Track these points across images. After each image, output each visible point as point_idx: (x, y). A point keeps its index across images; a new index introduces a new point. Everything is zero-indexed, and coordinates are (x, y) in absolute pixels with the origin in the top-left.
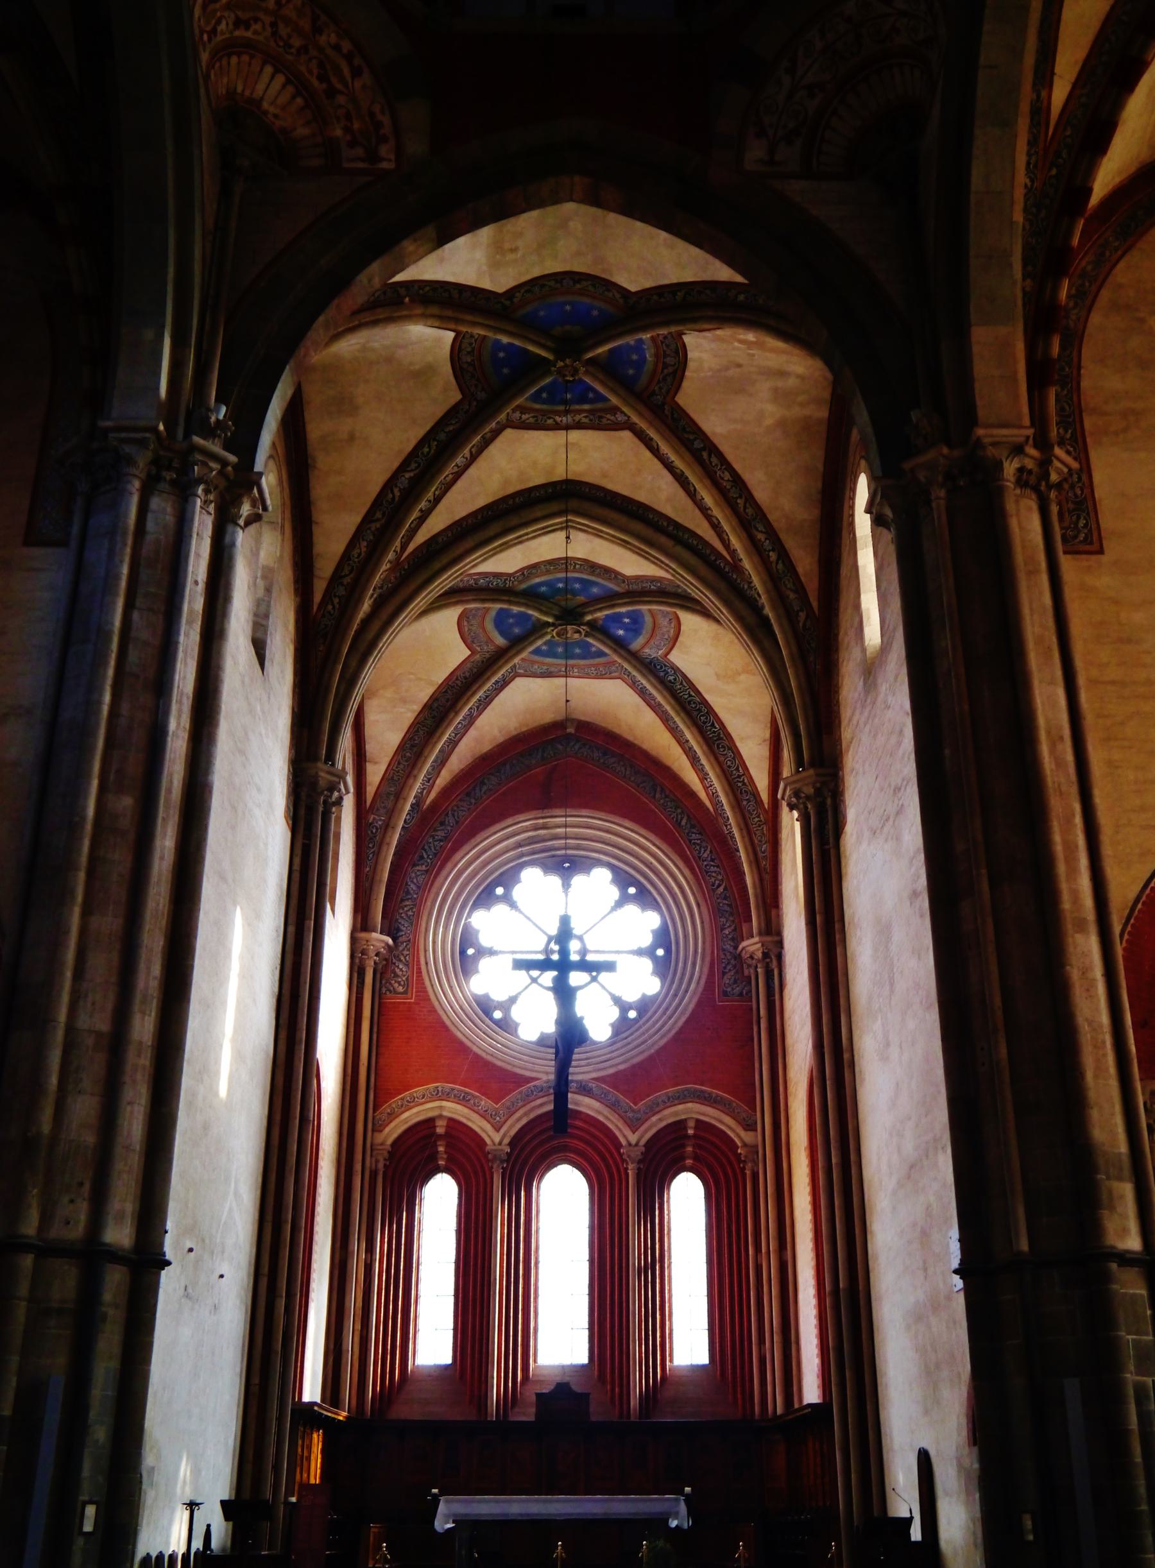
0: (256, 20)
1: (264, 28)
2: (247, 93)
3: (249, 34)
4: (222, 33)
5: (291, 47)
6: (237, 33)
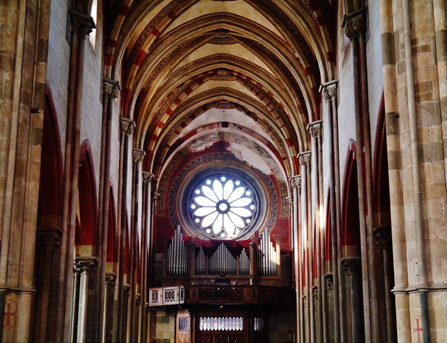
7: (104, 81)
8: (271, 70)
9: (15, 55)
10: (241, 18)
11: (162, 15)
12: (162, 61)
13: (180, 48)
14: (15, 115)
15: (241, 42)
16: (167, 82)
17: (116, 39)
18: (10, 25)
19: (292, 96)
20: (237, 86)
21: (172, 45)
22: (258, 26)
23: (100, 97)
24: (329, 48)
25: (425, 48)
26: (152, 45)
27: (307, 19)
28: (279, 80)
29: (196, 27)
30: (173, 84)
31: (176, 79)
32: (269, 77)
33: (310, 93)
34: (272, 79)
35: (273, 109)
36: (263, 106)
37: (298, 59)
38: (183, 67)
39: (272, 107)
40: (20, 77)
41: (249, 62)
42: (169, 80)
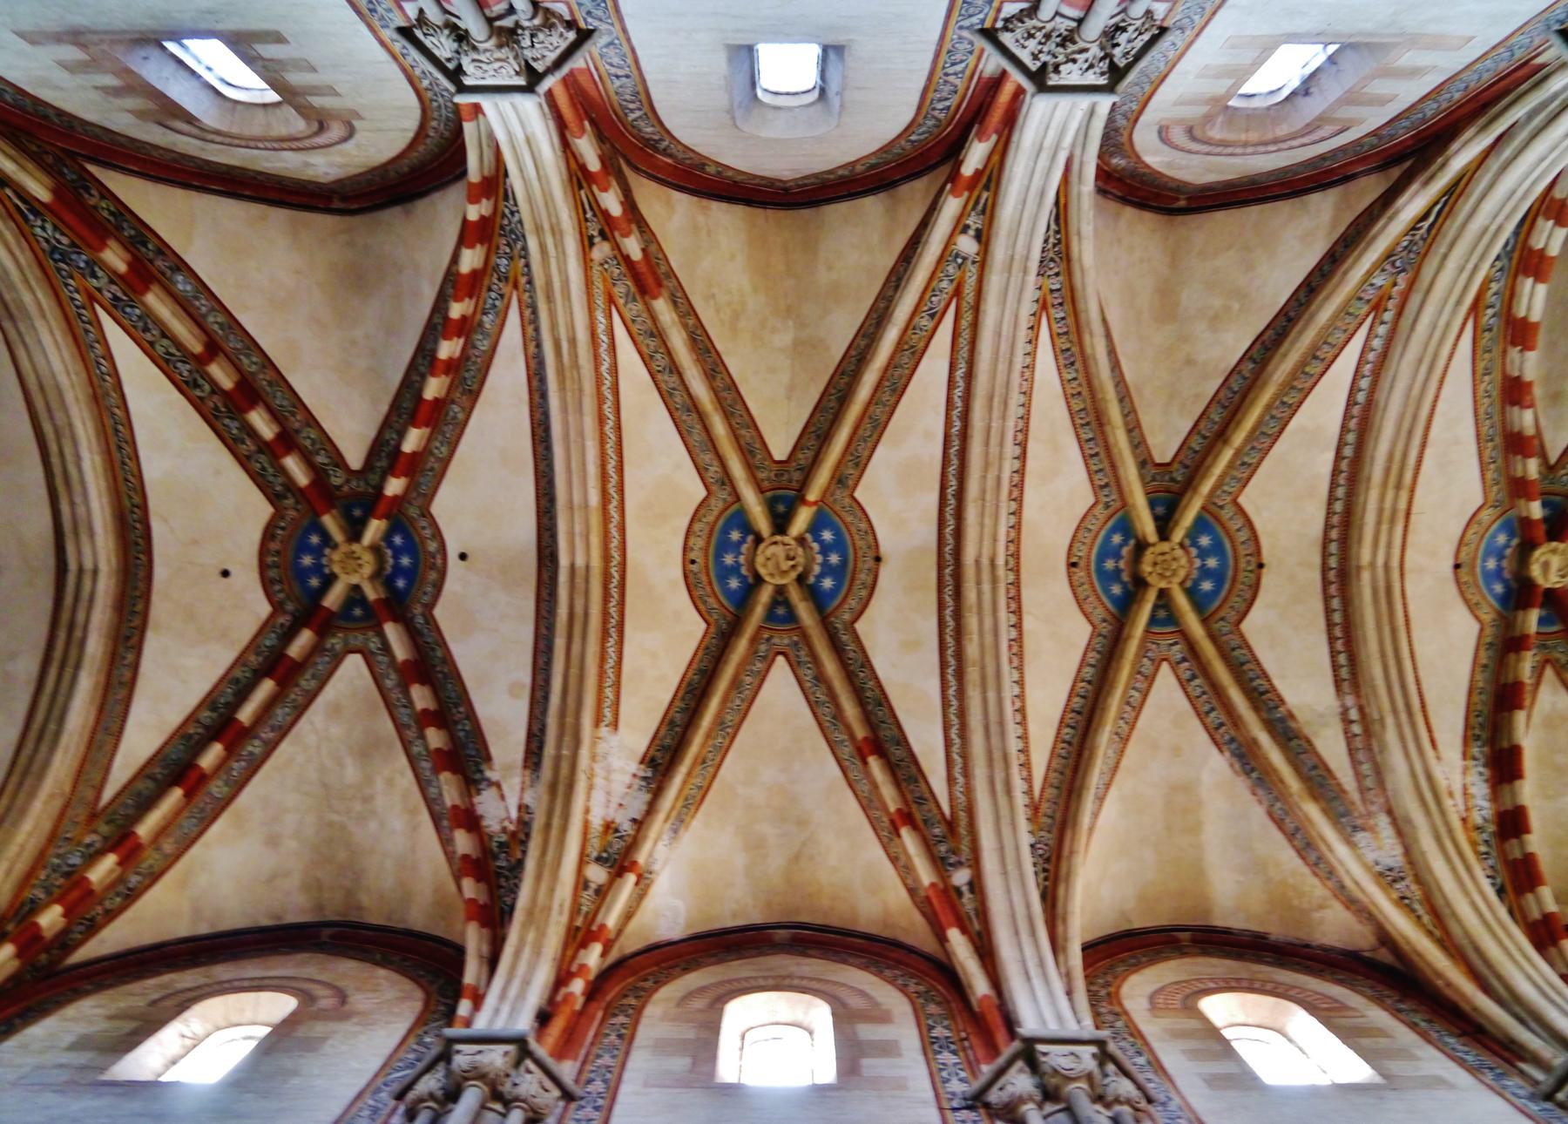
10: (950, 491)
12: (1279, 824)
13: (1232, 740)
22: (958, 424)
38: (1349, 737)
42: (1390, 812)
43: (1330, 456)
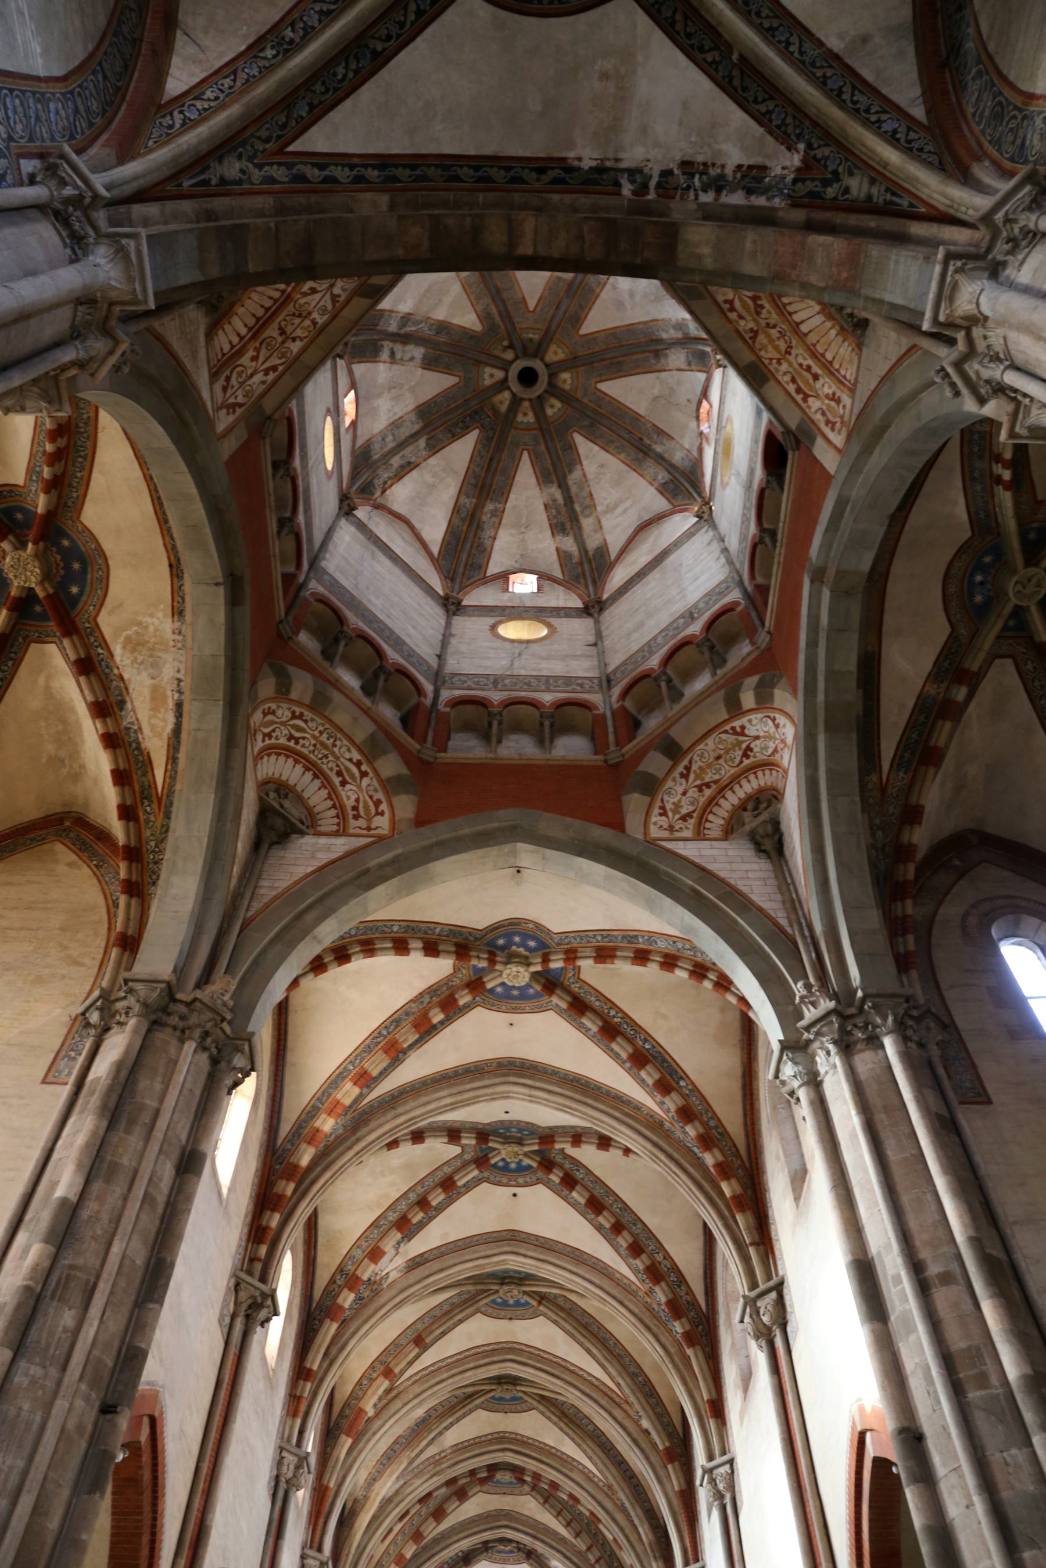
0: (801, 365)
1: (797, 356)
2: (829, 324)
3: (810, 362)
4: (830, 387)
5: (780, 332)
6: (819, 372)
7: (282, 1449)
8: (596, 1465)
9: (98, 1277)
10: (541, 1353)
11: (404, 1342)
12: (395, 1442)
14: (61, 1405)
15: (541, 1407)
16: (402, 1487)
17: (315, 1367)
18: (105, 1217)
19: (637, 1522)
20: (530, 1506)
21: (416, 1401)
22: (572, 1368)
23: (269, 1483)
24: (709, 1391)
25: (946, 1278)
26: (380, 1399)
27: (663, 1339)
28: (610, 1487)
29: (461, 1369)
30: (411, 1493)
31: (418, 1482)
32: (591, 1480)
33: (676, 1502)
34: (596, 1485)
35: (600, 1558)
36: (579, 1553)
37: (647, 1432)
38: (433, 1457)
39: (598, 1554)
40: (96, 1323)
41: (553, 1451)
42: (405, 1483)
43: (552, 1444)
